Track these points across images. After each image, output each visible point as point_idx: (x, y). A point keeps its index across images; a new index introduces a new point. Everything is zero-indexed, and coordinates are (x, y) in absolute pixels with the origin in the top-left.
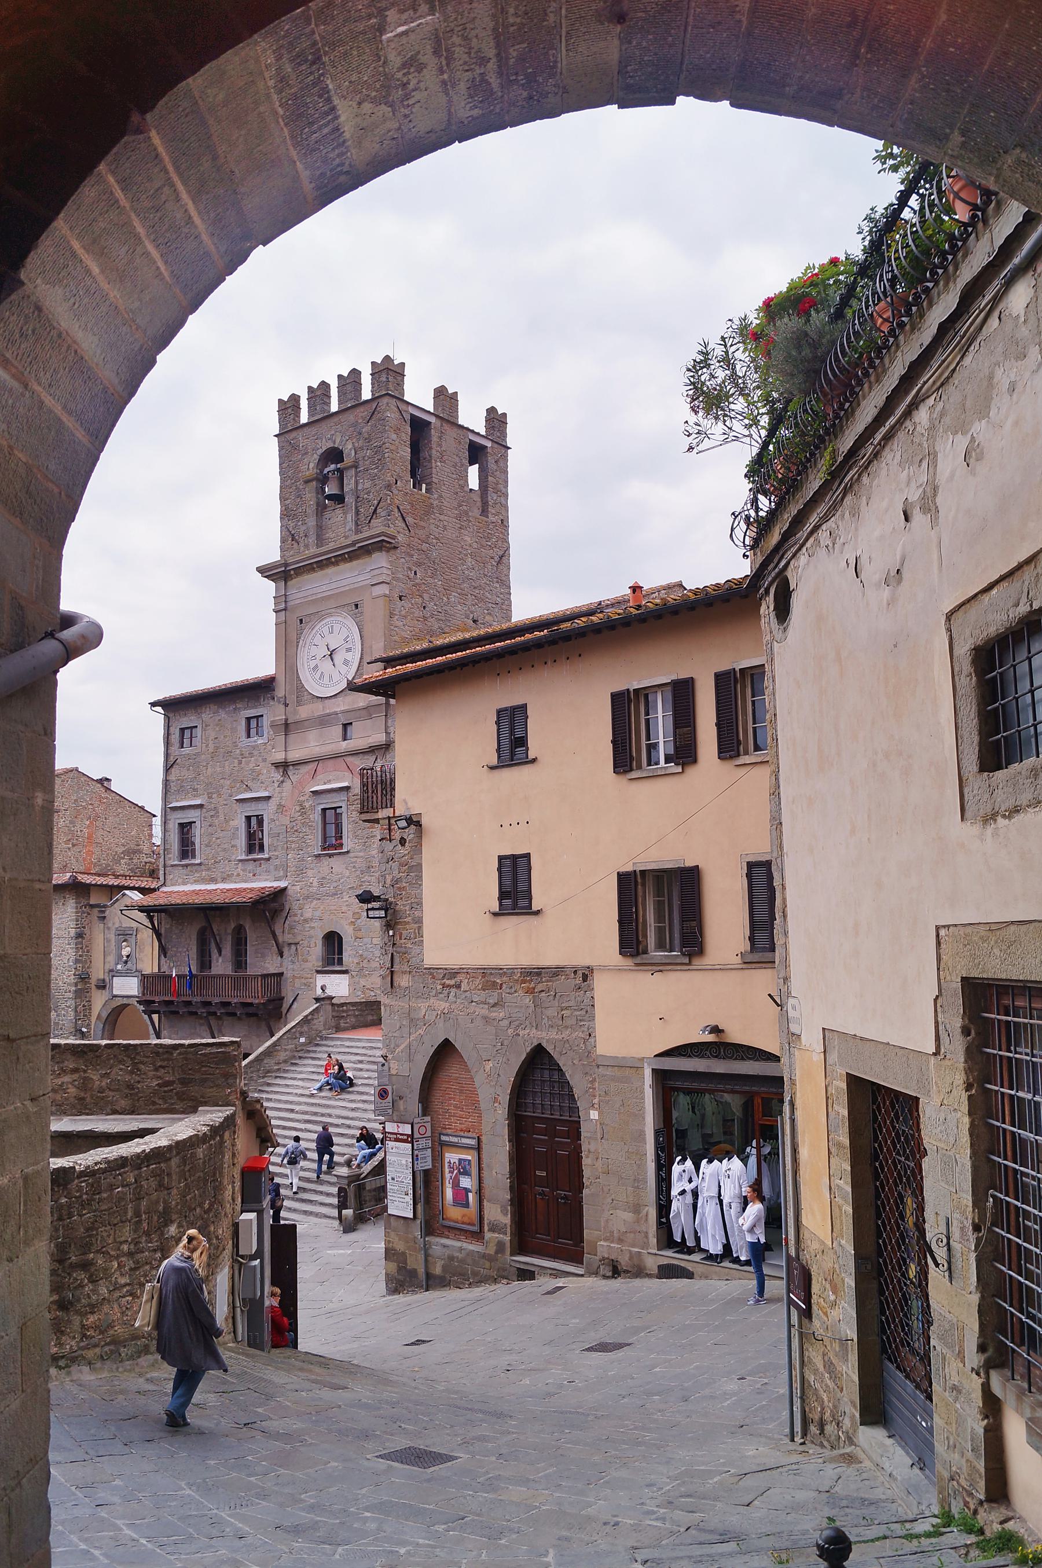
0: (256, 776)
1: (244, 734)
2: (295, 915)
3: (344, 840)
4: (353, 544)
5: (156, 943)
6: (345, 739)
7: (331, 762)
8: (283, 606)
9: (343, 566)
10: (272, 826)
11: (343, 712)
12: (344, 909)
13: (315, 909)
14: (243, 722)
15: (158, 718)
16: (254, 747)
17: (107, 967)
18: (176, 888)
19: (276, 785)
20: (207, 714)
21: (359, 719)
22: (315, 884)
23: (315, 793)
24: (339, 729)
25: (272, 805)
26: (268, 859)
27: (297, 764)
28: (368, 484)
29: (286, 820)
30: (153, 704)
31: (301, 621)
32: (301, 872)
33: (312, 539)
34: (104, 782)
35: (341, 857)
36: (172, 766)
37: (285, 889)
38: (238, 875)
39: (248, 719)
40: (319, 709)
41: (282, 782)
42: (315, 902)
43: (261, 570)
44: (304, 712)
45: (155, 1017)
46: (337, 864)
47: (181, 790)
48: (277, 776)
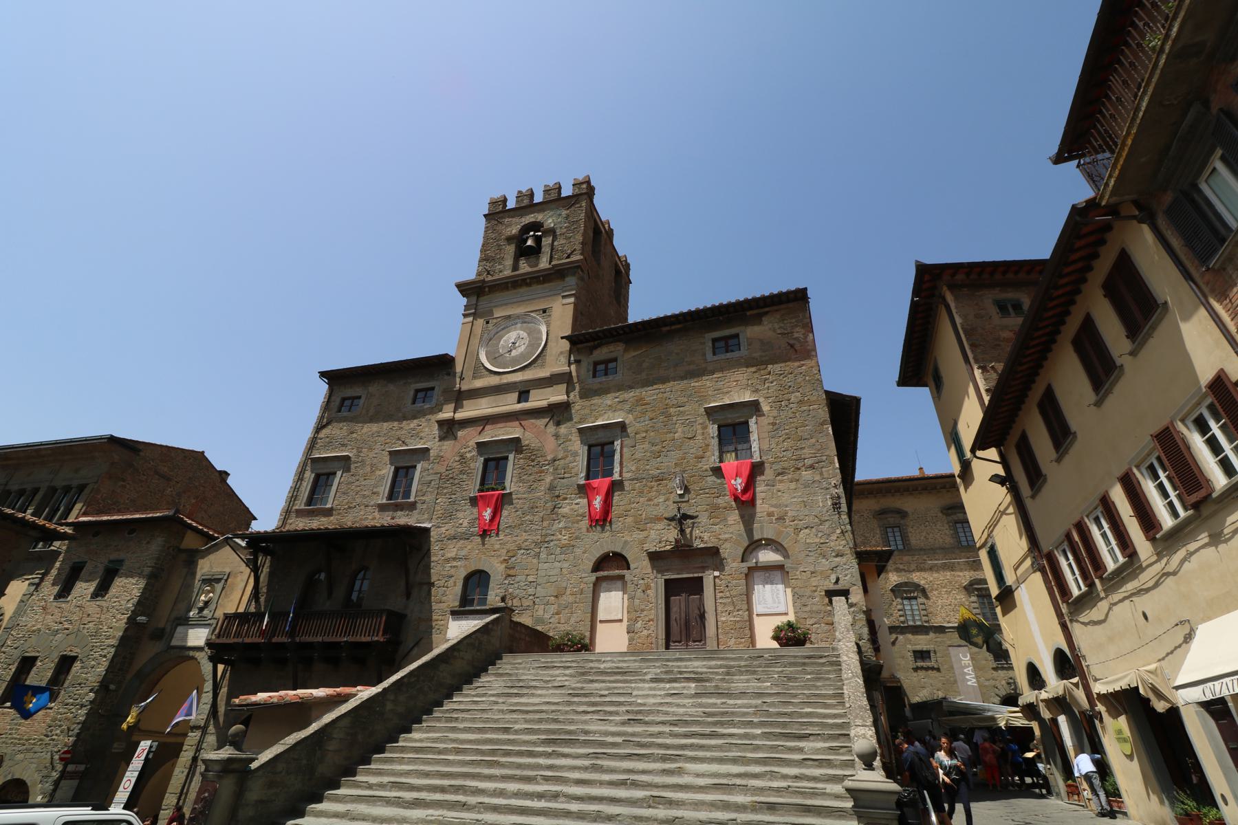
1: (410, 401)
2: (436, 555)
3: (507, 484)
5: (252, 581)
6: (519, 402)
9: (534, 287)
12: (497, 547)
14: (412, 393)
15: (323, 387)
22: (465, 524)
24: (516, 395)
30: (323, 374)
32: (449, 516)
34: (224, 475)
36: (324, 427)
37: (427, 530)
39: (417, 391)
40: (494, 381)
43: (459, 286)
44: (478, 384)
45: (221, 667)
47: (329, 445)
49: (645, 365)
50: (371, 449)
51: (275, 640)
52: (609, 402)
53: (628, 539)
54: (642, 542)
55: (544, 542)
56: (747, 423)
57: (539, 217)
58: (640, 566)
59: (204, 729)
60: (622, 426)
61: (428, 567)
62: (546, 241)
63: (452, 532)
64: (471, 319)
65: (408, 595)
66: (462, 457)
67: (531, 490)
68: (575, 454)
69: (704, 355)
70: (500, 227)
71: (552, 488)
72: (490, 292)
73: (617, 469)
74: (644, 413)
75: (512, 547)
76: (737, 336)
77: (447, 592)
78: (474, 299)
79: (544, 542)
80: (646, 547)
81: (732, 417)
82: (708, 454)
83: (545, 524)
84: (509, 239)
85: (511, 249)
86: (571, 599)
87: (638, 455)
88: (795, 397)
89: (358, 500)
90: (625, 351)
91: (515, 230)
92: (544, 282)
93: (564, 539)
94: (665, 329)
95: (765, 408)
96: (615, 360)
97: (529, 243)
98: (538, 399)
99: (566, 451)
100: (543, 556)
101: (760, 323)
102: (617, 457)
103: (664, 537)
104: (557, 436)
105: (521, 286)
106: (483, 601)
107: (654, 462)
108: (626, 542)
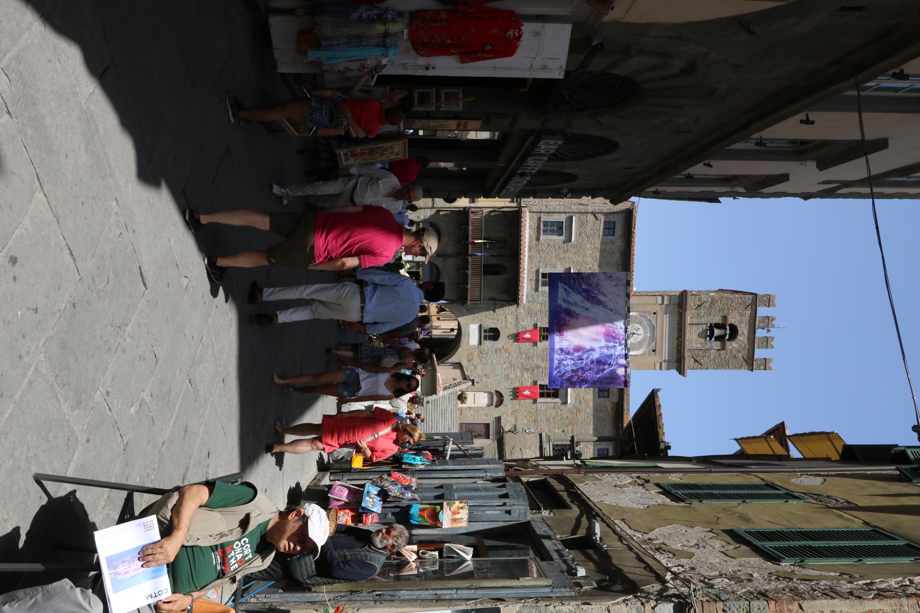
4: (684, 358)
9: (676, 342)
18: (528, 218)
20: (619, 243)
22: (524, 323)
26: (537, 290)
28: (712, 356)
32: (530, 312)
33: (695, 321)
47: (582, 224)
49: (600, 414)
50: (575, 254)
51: (470, 246)
54: (506, 413)
55: (512, 366)
57: (743, 337)
59: (433, 207)
60: (565, 403)
61: (502, 306)
62: (717, 345)
67: (538, 356)
70: (742, 307)
71: (538, 367)
74: (572, 413)
75: (510, 349)
77: (490, 319)
78: (677, 301)
79: (512, 366)
84: (725, 318)
85: (718, 320)
89: (543, 256)
90: (613, 403)
91: (732, 320)
93: (512, 376)
96: (608, 397)
100: (504, 366)
102: (549, 400)
106: (485, 338)
107: (544, 418)
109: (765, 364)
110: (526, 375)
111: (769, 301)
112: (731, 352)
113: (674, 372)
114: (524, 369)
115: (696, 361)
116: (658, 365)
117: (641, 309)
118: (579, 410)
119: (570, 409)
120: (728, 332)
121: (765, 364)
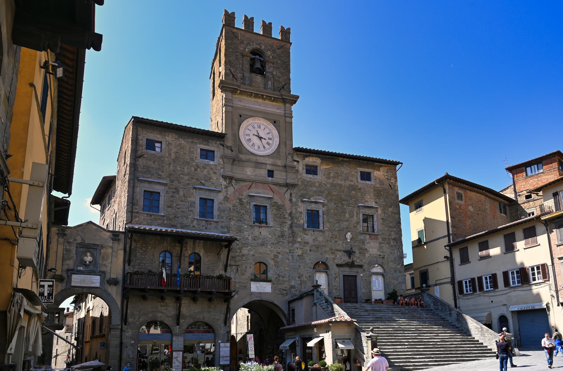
0: (208, 179)
2: (237, 252)
7: (261, 185)
8: (231, 104)
10: (221, 206)
11: (270, 164)
13: (249, 250)
16: (207, 165)
17: (65, 267)
19: (223, 187)
21: (278, 170)
22: (250, 238)
23: (250, 196)
25: (221, 196)
26: (217, 222)
27: (238, 180)
29: (230, 205)
31: (240, 116)
35: (267, 229)
38: (194, 226)
41: (227, 187)
42: (249, 247)
44: (242, 157)
46: (264, 232)
48: (224, 183)
49: (331, 175)
52: (314, 189)
53: (327, 256)
54: (334, 259)
56: (373, 216)
58: (334, 270)
59: (122, 330)
62: (269, 68)
63: (244, 242)
64: (230, 109)
65: (226, 271)
66: (240, 199)
68: (301, 213)
69: (357, 178)
71: (291, 226)
72: (240, 94)
73: (321, 225)
75: (275, 253)
76: (370, 173)
80: (336, 261)
81: (368, 212)
82: (358, 226)
83: (290, 245)
86: (305, 279)
87: (331, 220)
88: (390, 209)
92: (273, 101)
93: (300, 252)
94: (341, 159)
95: (380, 211)
97: (258, 65)
98: (279, 176)
99: (296, 209)
101: (379, 170)
102: (321, 219)
103: (345, 259)
104: (291, 200)
105: (259, 98)
107: (337, 225)
108: (327, 258)
109: (286, 33)
110: (299, 240)
111: (229, 18)
112: (275, 58)
113: (294, 107)
114: (294, 242)
115: (283, 87)
116: (288, 120)
117: (237, 127)
118: (329, 194)
119: (328, 201)
120: (257, 57)
121: (286, 33)
